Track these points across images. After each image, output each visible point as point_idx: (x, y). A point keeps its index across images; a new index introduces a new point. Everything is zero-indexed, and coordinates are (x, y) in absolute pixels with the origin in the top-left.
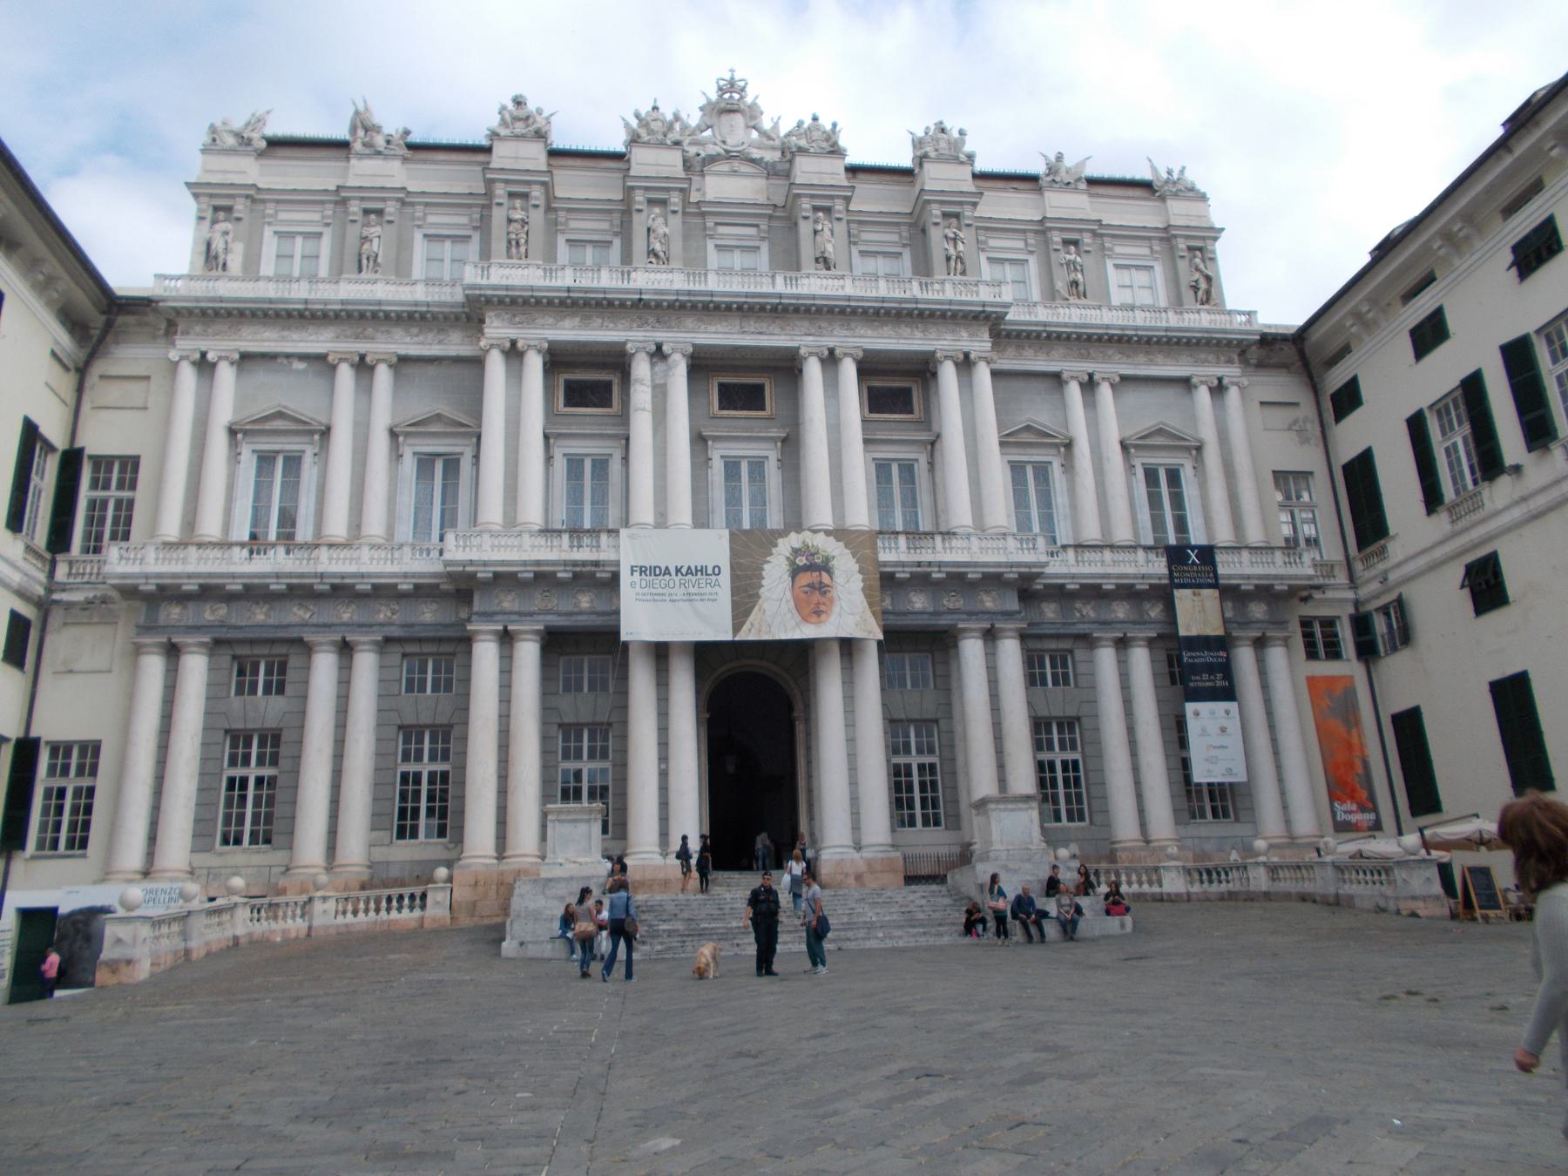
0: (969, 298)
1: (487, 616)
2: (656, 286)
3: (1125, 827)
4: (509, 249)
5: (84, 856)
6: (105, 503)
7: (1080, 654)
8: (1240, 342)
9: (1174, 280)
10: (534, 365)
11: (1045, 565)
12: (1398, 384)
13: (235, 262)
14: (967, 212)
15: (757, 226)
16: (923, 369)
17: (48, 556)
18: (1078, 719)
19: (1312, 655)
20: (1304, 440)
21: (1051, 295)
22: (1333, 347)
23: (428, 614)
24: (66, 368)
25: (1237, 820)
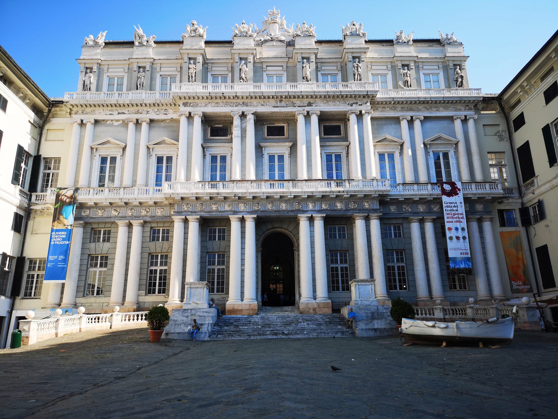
0: (362, 89)
1: (179, 213)
2: (242, 90)
4: (189, 78)
5: (39, 298)
6: (49, 174)
7: (405, 225)
8: (474, 101)
9: (447, 79)
11: (389, 191)
14: (363, 56)
15: (282, 66)
17: (29, 193)
18: (404, 250)
19: (503, 224)
20: (501, 138)
21: (396, 86)
22: (513, 101)
23: (159, 212)
24: (36, 127)
25: (469, 290)
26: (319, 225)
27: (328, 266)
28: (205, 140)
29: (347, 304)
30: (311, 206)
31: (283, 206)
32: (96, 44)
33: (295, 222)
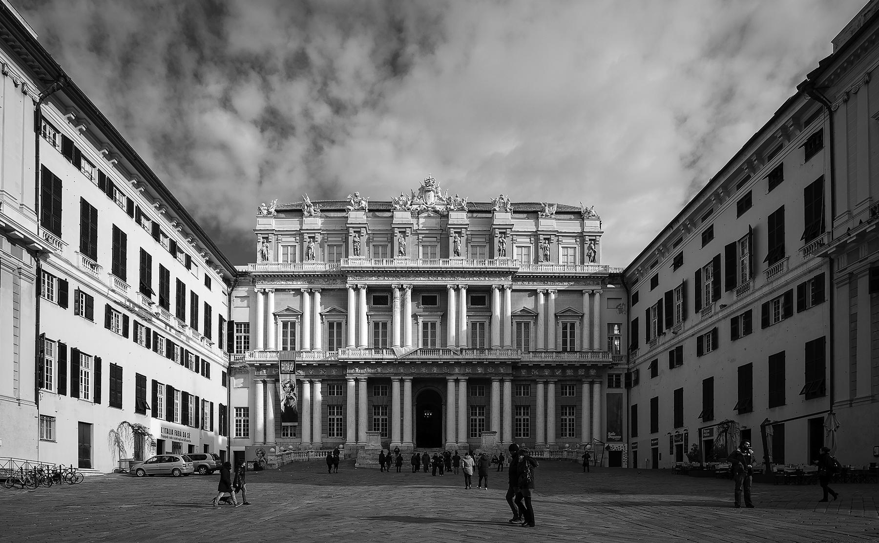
3: (540, 439)
10: (364, 292)
12: (649, 298)
13: (271, 256)
16: (489, 290)
23: (334, 372)
26: (463, 386)
27: (468, 418)
28: (370, 309)
29: (479, 447)
30: (457, 370)
31: (435, 370)
32: (269, 213)
33: (444, 382)
